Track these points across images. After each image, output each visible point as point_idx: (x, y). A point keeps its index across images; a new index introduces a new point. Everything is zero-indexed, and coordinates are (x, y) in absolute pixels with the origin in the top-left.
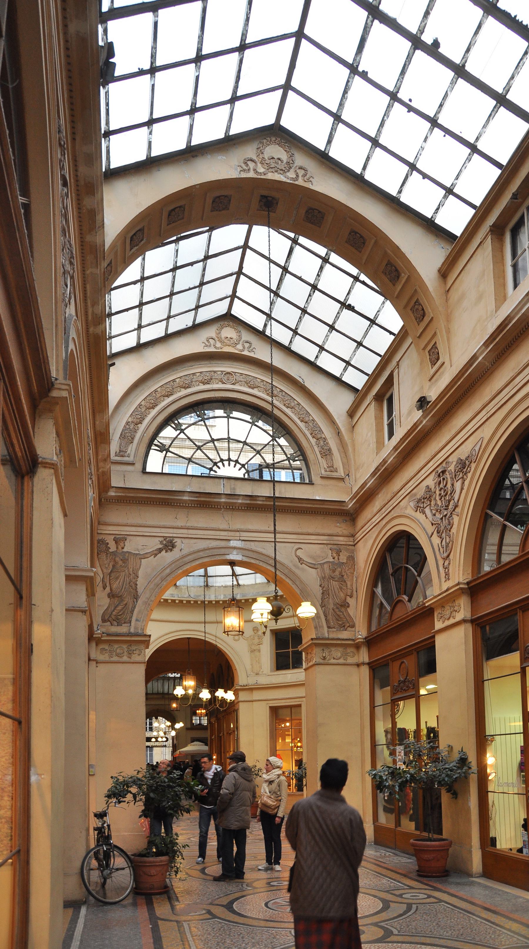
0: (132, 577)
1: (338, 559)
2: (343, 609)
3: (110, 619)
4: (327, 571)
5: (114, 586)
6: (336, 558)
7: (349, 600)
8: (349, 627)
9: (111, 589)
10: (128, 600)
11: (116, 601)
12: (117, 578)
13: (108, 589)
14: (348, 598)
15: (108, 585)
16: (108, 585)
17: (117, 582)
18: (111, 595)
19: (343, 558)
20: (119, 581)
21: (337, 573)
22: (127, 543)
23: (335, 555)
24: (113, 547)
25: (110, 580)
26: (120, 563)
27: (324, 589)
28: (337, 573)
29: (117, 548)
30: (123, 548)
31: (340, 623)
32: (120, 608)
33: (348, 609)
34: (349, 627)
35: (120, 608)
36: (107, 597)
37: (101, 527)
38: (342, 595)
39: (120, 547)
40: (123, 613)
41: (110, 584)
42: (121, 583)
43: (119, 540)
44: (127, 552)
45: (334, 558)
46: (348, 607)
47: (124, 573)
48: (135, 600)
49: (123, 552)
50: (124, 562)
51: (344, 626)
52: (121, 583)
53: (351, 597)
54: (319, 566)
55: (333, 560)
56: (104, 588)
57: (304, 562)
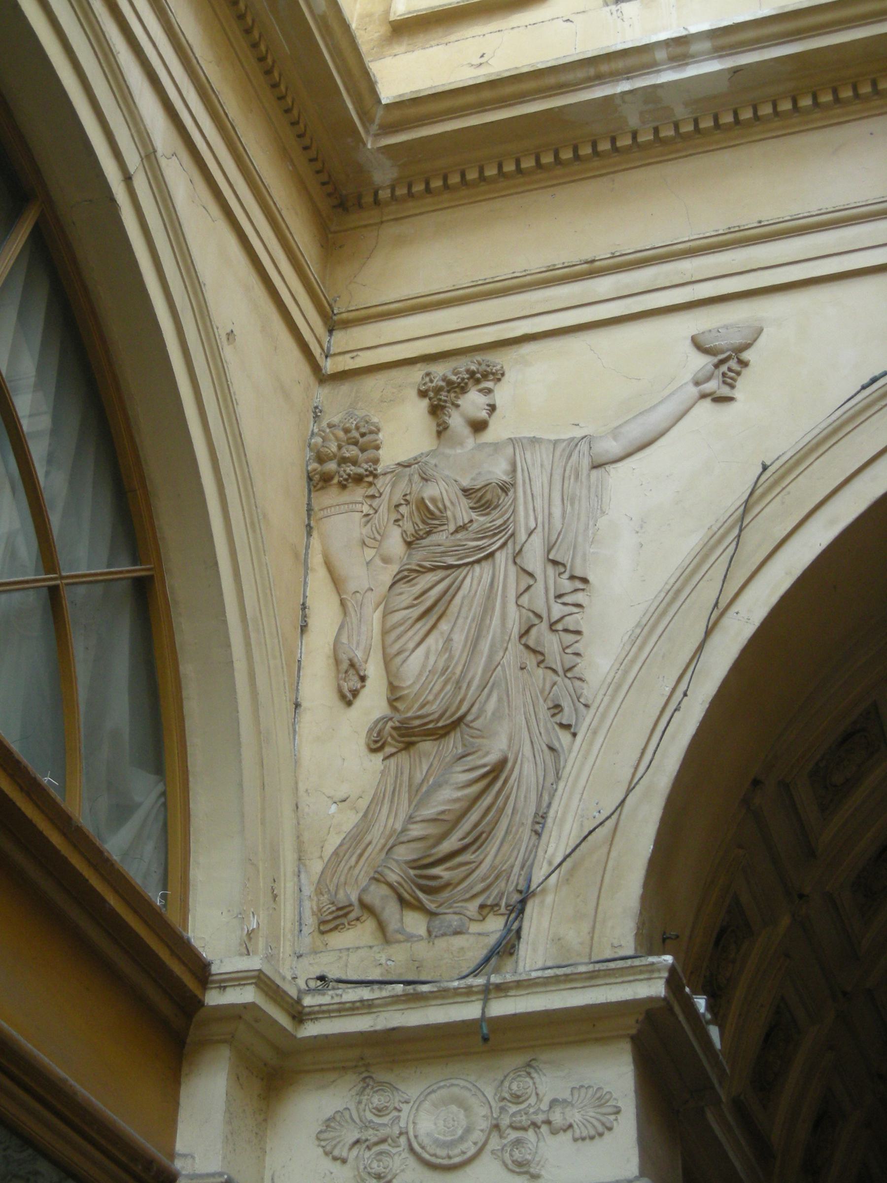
0: (539, 587)
3: (378, 895)
5: (414, 666)
9: (393, 702)
12: (433, 612)
13: (373, 703)
15: (374, 670)
16: (374, 670)
20: (444, 626)
22: (502, 394)
24: (403, 431)
25: (385, 633)
26: (461, 511)
29: (442, 430)
30: (478, 426)
35: (446, 798)
36: (359, 744)
37: (341, 340)
39: (456, 421)
40: (476, 841)
41: (387, 661)
42: (459, 639)
43: (455, 384)
47: (482, 572)
48: (565, 737)
49: (481, 447)
52: (459, 639)
56: (348, 698)
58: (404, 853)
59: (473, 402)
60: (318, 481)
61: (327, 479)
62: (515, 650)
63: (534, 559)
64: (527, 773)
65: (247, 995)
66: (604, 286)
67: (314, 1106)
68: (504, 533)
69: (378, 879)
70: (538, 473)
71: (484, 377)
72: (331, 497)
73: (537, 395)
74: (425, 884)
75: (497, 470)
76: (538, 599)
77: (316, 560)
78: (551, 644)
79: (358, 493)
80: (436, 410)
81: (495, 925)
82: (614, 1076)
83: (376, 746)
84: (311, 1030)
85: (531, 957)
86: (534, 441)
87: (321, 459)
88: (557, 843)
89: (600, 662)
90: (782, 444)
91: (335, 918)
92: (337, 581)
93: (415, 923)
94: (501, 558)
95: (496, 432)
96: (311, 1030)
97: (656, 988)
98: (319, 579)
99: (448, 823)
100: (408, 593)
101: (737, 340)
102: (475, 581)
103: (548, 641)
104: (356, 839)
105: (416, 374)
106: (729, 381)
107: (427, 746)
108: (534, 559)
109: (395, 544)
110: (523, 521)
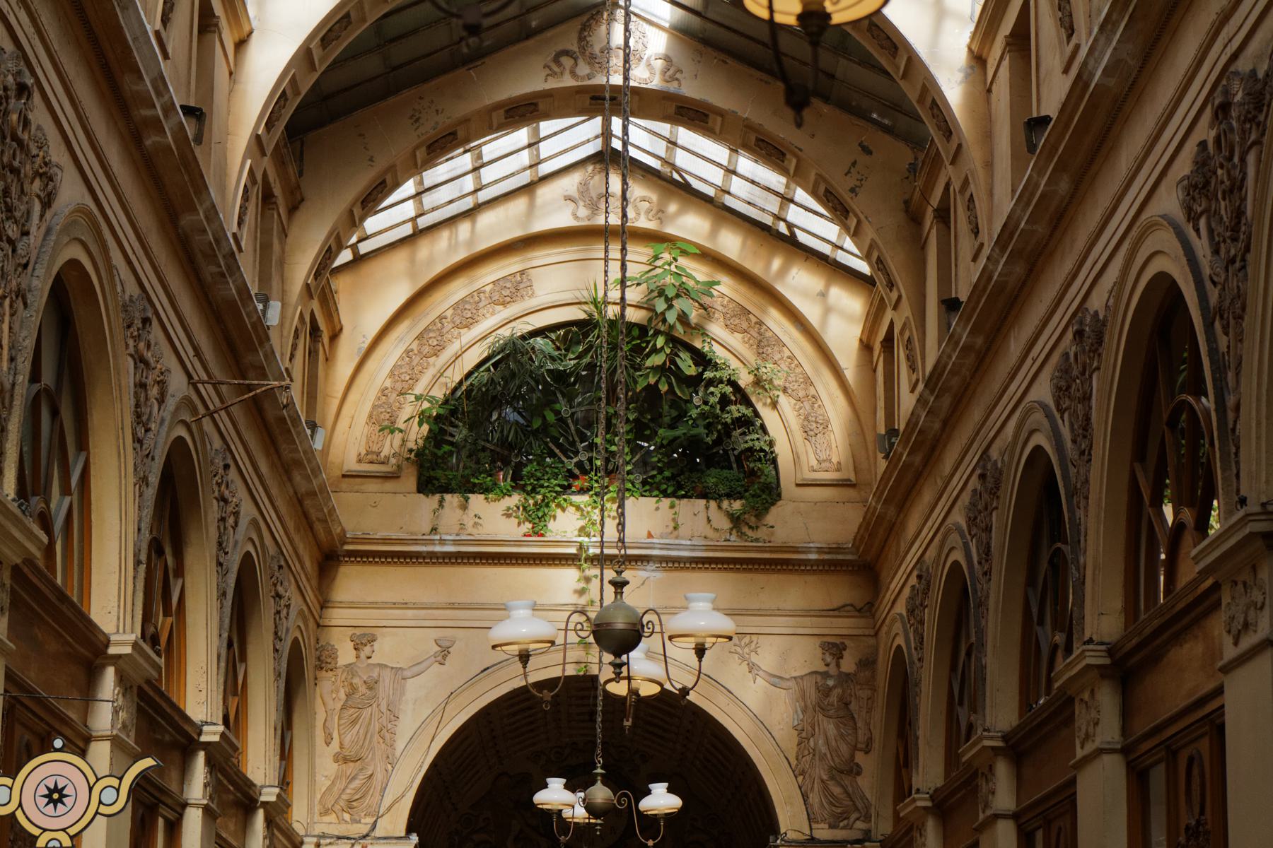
1: (838, 665)
6: (833, 665)
7: (860, 758)
10: (377, 766)
11: (351, 768)
12: (354, 722)
14: (860, 758)
16: (335, 735)
17: (355, 731)
18: (342, 758)
19: (848, 665)
20: (357, 727)
23: (829, 659)
26: (363, 689)
27: (804, 735)
28: (834, 698)
31: (839, 810)
32: (356, 784)
33: (859, 780)
34: (858, 819)
38: (844, 749)
39: (363, 655)
43: (363, 641)
44: (379, 665)
45: (827, 665)
46: (859, 773)
50: (370, 688)
53: (867, 751)
55: (825, 669)
56: (328, 744)
58: (345, 797)
59: (367, 650)
62: (376, 737)
64: (379, 776)
66: (410, 613)
70: (387, 676)
71: (372, 640)
73: (387, 649)
74: (350, 806)
75: (375, 675)
76: (384, 721)
78: (388, 736)
79: (331, 673)
81: (370, 820)
85: (378, 832)
86: (386, 666)
88: (387, 801)
89: (400, 745)
93: (347, 817)
99: (357, 790)
100: (347, 713)
101: (448, 644)
102: (366, 713)
103: (387, 734)
104: (329, 789)
105: (350, 631)
106: (444, 657)
107: (351, 764)
108: (384, 708)
109: (342, 696)
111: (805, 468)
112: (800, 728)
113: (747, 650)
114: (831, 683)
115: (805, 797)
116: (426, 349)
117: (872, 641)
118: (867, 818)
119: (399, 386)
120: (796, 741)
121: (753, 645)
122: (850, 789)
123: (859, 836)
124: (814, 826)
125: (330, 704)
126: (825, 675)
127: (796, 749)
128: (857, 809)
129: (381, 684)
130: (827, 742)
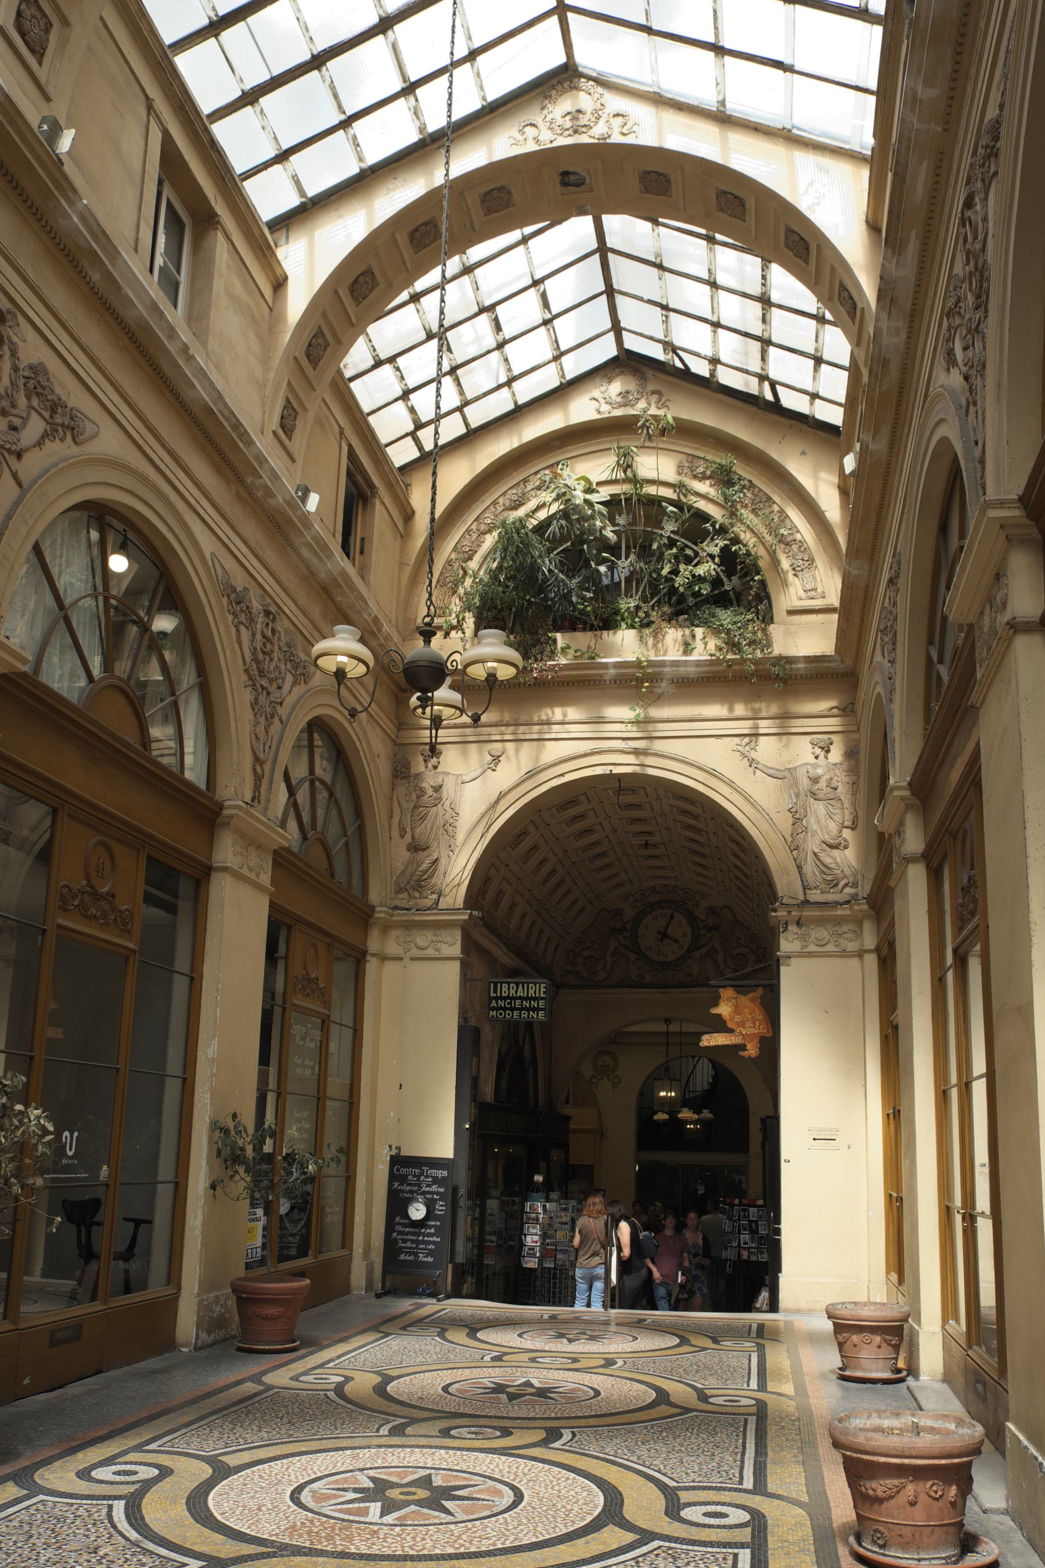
1: (826, 758)
2: (836, 853)
3: (409, 887)
4: (804, 783)
8: (846, 885)
13: (408, 838)
16: (408, 830)
21: (822, 784)
22: (442, 759)
23: (818, 751)
26: (430, 792)
27: (797, 816)
29: (426, 767)
30: (435, 767)
39: (430, 765)
40: (431, 876)
42: (429, 827)
44: (444, 773)
45: (817, 757)
51: (836, 885)
52: (429, 827)
54: (786, 773)
56: (402, 837)
57: (759, 766)
58: (414, 878)
59: (434, 761)
60: (395, 777)
61: (397, 777)
63: (447, 806)
65: (382, 915)
67: (394, 933)
68: (440, 799)
69: (408, 883)
72: (398, 781)
76: (447, 817)
77: (395, 798)
78: (450, 829)
80: (425, 761)
81: (435, 896)
82: (458, 934)
83: (408, 850)
84: (395, 918)
87: (396, 770)
89: (460, 837)
90: (505, 786)
91: (399, 891)
92: (400, 805)
93: (417, 894)
94: (440, 806)
95: (440, 769)
96: (395, 918)
97: (466, 917)
98: (395, 802)
103: (448, 828)
104: (404, 872)
110: (444, 796)
111: (794, 598)
112: (793, 810)
113: (747, 748)
114: (820, 771)
115: (799, 868)
116: (483, 528)
117: (855, 736)
118: (855, 885)
119: (461, 556)
120: (791, 821)
121: (753, 744)
122: (839, 859)
123: (848, 898)
124: (808, 892)
125: (405, 805)
126: (815, 766)
127: (791, 828)
128: (845, 877)
129: (444, 788)
130: (818, 821)
